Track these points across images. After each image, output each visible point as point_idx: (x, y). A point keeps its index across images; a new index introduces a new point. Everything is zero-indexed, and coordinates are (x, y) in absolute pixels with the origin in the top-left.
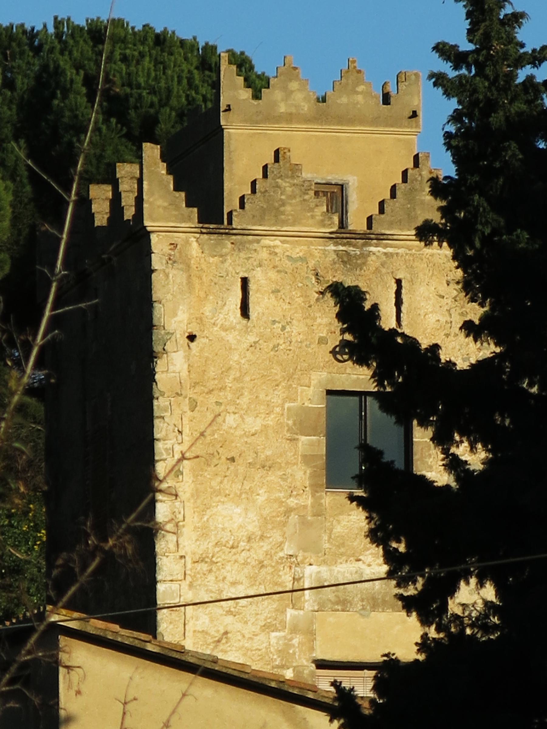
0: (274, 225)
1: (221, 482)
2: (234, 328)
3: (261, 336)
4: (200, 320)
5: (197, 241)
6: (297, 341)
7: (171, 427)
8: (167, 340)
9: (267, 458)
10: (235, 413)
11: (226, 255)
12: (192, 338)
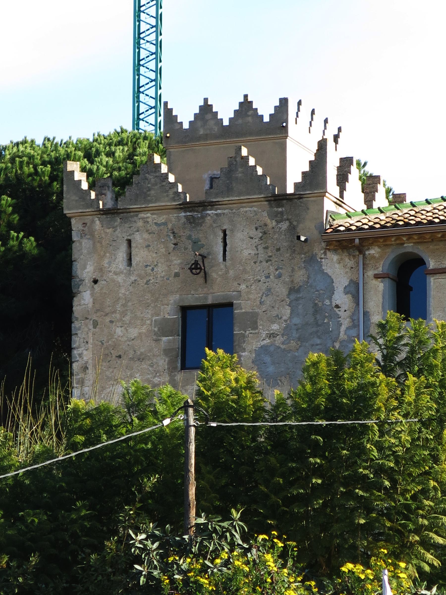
0: (143, 204)
1: (113, 372)
2: (122, 272)
3: (139, 275)
4: (101, 270)
5: (99, 220)
6: (161, 277)
7: (82, 340)
8: (80, 284)
9: (142, 354)
10: (121, 327)
11: (117, 226)
12: (95, 282)
